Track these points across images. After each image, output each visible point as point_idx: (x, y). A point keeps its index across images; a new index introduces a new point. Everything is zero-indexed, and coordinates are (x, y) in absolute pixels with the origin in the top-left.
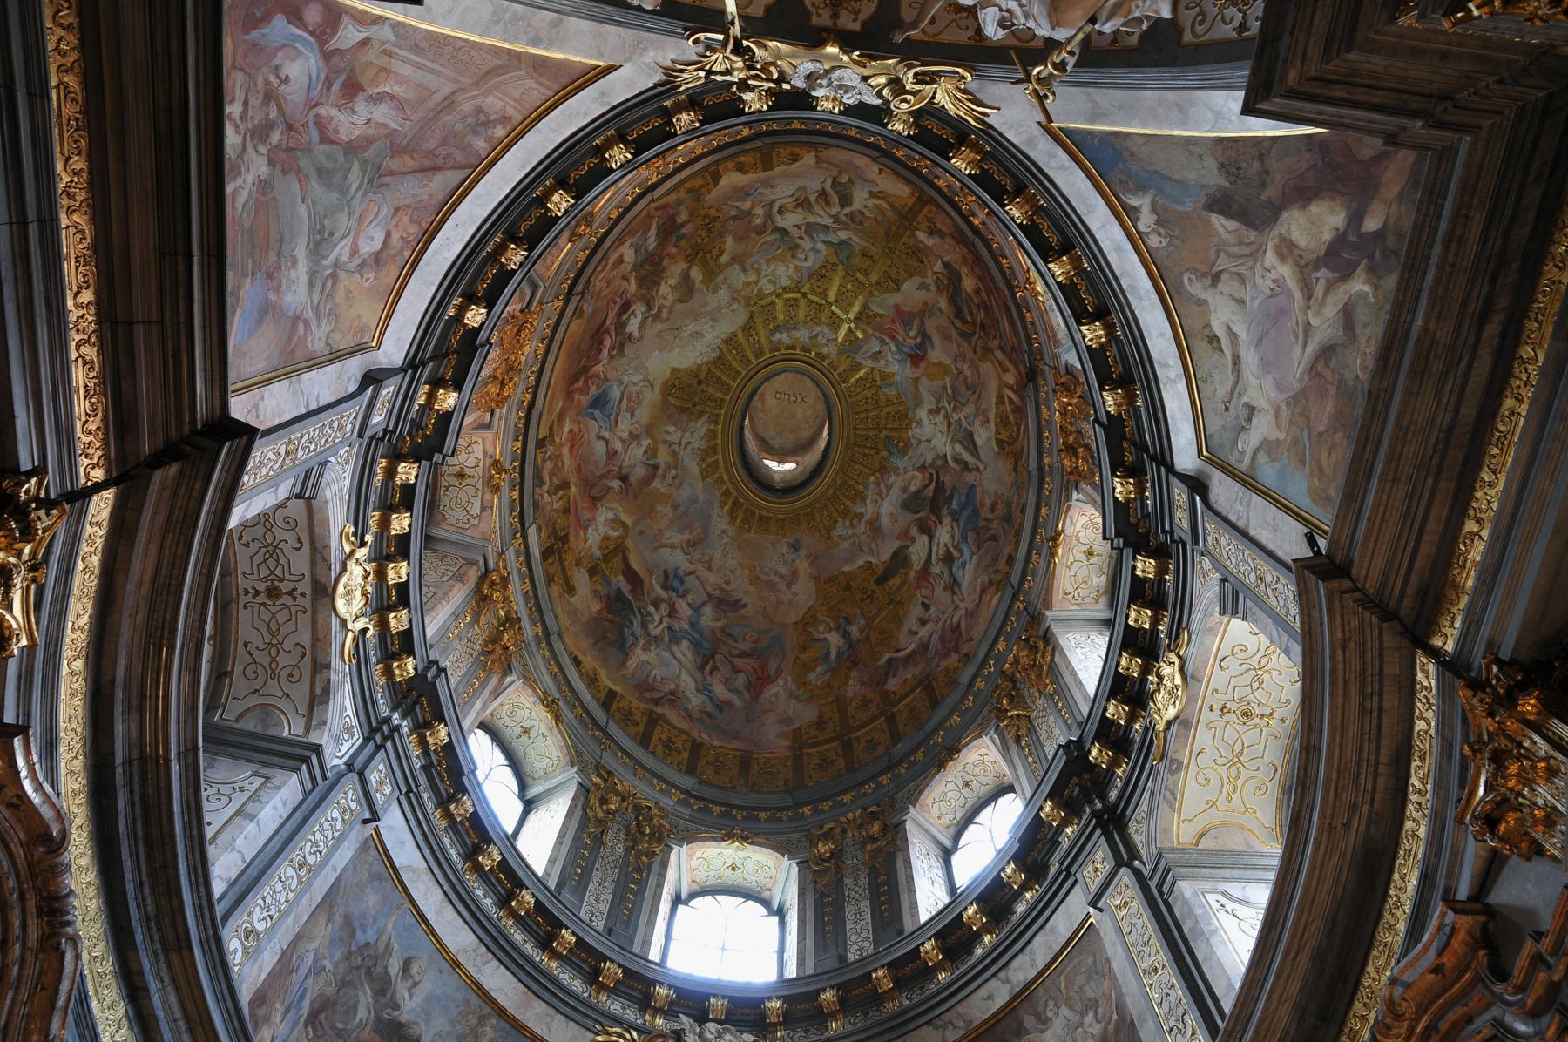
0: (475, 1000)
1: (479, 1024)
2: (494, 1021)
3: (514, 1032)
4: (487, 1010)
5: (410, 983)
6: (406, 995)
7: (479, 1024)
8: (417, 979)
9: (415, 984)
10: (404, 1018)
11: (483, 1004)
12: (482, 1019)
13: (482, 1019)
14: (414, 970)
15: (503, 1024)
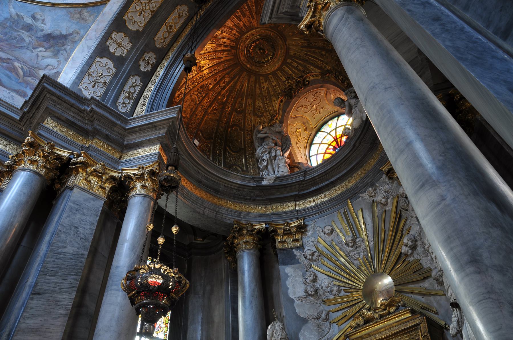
0: (72, 10)
1: (81, 15)
2: (85, 10)
3: (96, 8)
4: (79, 9)
5: (40, 21)
6: (43, 25)
7: (81, 15)
8: (43, 18)
9: (43, 20)
10: (49, 32)
11: (76, 9)
12: (80, 13)
13: (80, 13)
14: (38, 17)
15: (89, 9)
